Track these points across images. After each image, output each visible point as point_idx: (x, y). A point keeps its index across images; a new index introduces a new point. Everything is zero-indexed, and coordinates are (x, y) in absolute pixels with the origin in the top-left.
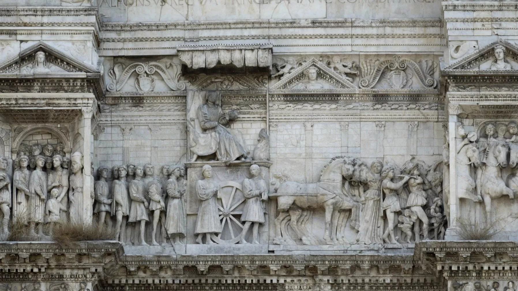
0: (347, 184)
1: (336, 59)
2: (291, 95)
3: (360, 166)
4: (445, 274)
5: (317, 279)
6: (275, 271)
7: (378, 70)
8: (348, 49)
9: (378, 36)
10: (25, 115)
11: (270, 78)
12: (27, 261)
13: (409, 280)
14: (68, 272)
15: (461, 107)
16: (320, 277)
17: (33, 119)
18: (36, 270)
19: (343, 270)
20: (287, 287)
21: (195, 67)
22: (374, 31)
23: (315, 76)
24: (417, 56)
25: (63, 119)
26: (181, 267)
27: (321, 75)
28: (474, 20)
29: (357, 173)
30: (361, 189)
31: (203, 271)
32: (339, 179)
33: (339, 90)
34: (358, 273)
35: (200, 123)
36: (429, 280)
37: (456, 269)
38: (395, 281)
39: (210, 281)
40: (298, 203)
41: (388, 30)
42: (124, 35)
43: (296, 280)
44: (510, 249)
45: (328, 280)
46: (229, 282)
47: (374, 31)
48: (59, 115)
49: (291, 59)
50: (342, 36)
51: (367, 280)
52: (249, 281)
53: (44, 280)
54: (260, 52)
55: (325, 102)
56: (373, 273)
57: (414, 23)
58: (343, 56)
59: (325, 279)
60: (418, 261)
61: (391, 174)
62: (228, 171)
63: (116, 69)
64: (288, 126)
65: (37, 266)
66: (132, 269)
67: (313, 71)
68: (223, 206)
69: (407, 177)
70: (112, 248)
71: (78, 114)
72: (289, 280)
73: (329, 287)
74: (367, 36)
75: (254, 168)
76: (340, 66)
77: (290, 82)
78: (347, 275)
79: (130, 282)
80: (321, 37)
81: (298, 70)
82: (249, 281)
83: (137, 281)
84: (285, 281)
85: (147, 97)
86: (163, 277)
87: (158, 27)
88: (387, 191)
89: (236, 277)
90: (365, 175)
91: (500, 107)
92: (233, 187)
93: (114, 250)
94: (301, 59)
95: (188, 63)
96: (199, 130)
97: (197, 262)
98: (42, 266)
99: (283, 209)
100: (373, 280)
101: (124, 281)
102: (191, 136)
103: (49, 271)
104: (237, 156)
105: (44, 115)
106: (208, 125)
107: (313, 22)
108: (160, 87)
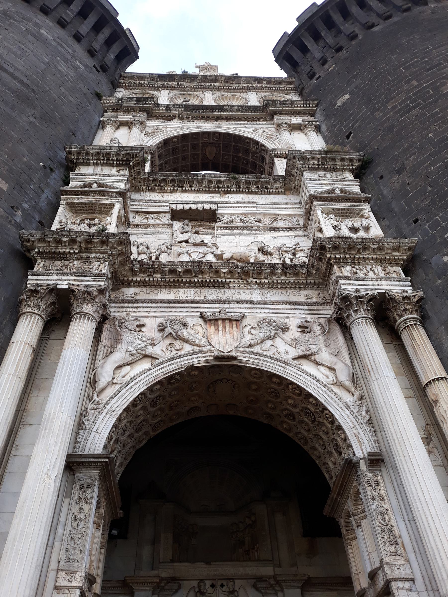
0: (261, 253)
1: (249, 216)
2: (228, 227)
3: (267, 246)
4: (332, 261)
5: (249, 280)
6: (224, 273)
7: (271, 220)
8: (256, 211)
9: (269, 208)
10: (82, 207)
11: (216, 222)
12: (67, 244)
13: (305, 282)
14: (93, 255)
15: (321, 208)
16: (251, 279)
17: (87, 210)
18: (72, 251)
19: (265, 273)
20: (231, 285)
21: (178, 209)
22: (268, 206)
23: (239, 221)
24: (290, 215)
25: (103, 211)
26: (167, 269)
27: (241, 221)
28: (321, 184)
29: (266, 248)
30: (269, 256)
31: (180, 272)
32: (257, 249)
33: (252, 225)
34: (274, 277)
35: (180, 231)
36: (317, 282)
37: (339, 256)
38: (296, 282)
39: (184, 280)
40: (234, 257)
41: (274, 206)
42: (141, 203)
43: (236, 281)
44: (372, 243)
45: (256, 281)
46: (196, 280)
47: (268, 206)
48: (101, 208)
49: (226, 215)
50: (252, 207)
51: (279, 281)
52: (208, 280)
53: (77, 259)
54: (211, 205)
55: (244, 230)
56: (283, 277)
57: (287, 204)
58: (253, 215)
59: (255, 280)
60: (310, 268)
61: (285, 246)
62: (195, 247)
63: (136, 216)
64: (226, 237)
65: (73, 249)
66: (137, 270)
67: (238, 220)
68: (192, 257)
69: (294, 247)
70: (123, 236)
71: (112, 206)
72: (232, 280)
73: (257, 286)
74: (264, 208)
75: (209, 244)
76: (251, 218)
77: (227, 223)
78: (267, 278)
79: (135, 279)
80: (241, 207)
81: (230, 219)
82: (208, 280)
83: (139, 279)
84: (230, 281)
85: (152, 225)
86: (155, 277)
87: (159, 201)
88: (283, 253)
89: (200, 278)
90: (270, 250)
91: (343, 209)
92: (197, 252)
93: (124, 238)
94: (232, 214)
95: (175, 209)
96: (178, 233)
97: (177, 265)
98: (76, 249)
99: (227, 258)
100: (283, 281)
101: (130, 279)
102: (175, 235)
103: (81, 254)
104: (200, 241)
105: (93, 207)
106: (184, 230)
107: (237, 202)
108: (158, 222)
